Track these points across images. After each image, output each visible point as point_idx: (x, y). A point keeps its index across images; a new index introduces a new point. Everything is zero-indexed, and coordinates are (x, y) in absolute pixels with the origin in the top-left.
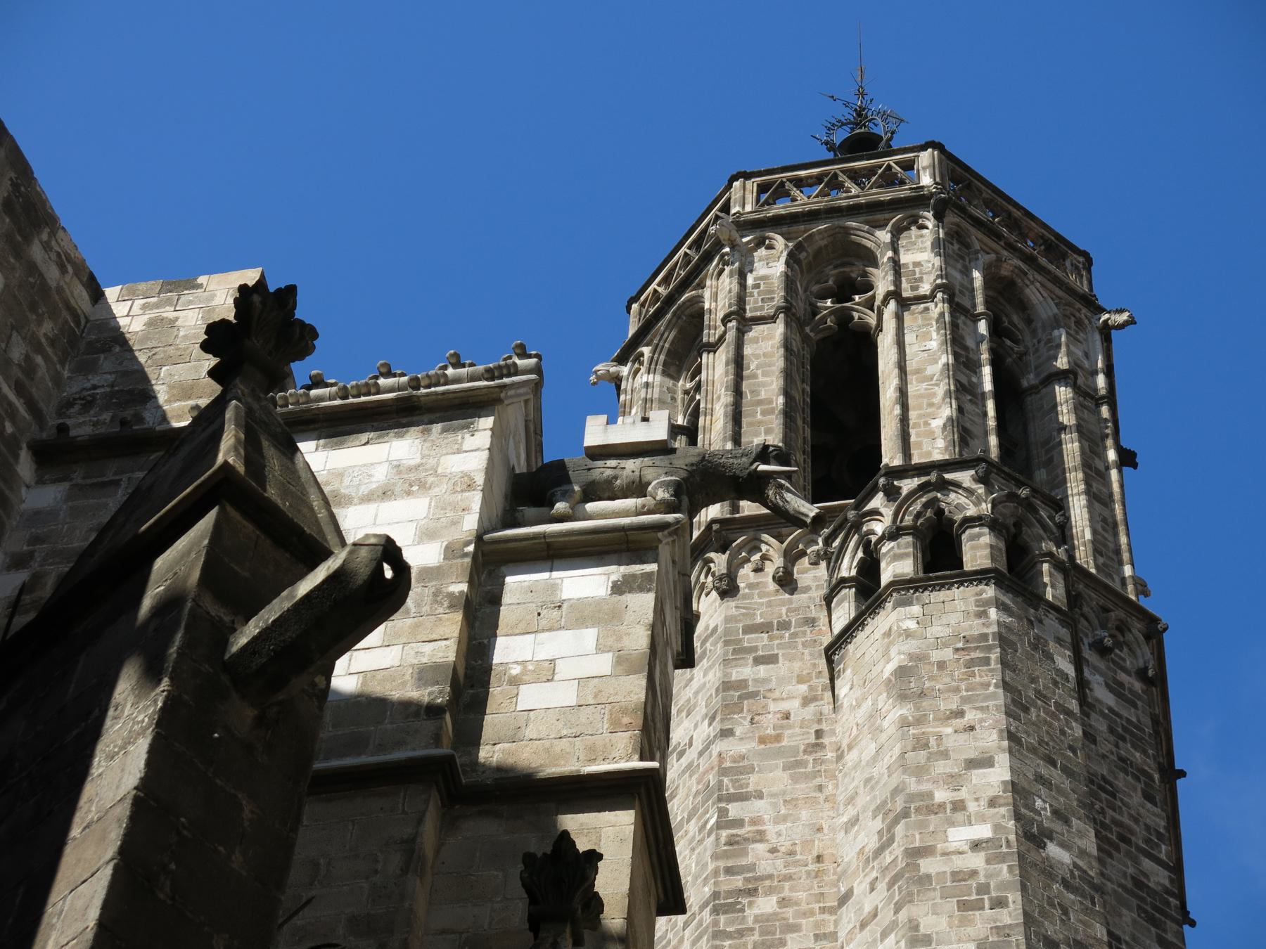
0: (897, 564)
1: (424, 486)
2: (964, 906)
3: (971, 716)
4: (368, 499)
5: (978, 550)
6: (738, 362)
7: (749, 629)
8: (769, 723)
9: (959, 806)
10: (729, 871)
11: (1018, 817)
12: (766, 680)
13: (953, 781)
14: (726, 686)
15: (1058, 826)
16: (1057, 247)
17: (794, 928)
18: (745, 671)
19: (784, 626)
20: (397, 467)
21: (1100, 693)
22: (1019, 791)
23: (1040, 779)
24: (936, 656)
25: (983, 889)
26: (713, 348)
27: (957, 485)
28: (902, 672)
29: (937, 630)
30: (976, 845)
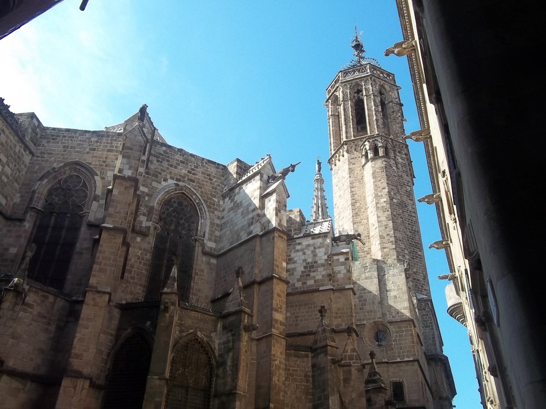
0: (370, 155)
1: (323, 247)
2: (384, 211)
3: (382, 181)
4: (318, 248)
5: (381, 152)
6: (344, 110)
7: (351, 159)
8: (355, 174)
9: (382, 196)
10: (353, 199)
11: (389, 197)
12: (354, 168)
13: (381, 191)
14: (349, 169)
15: (394, 196)
16: (389, 74)
17: (362, 208)
18: (351, 166)
19: (356, 158)
20: (321, 243)
21: (400, 160)
22: (389, 192)
23: (392, 189)
24: (378, 170)
25: (386, 209)
26: (340, 105)
27: (377, 140)
28: (373, 173)
29: (377, 166)
30: (384, 202)
